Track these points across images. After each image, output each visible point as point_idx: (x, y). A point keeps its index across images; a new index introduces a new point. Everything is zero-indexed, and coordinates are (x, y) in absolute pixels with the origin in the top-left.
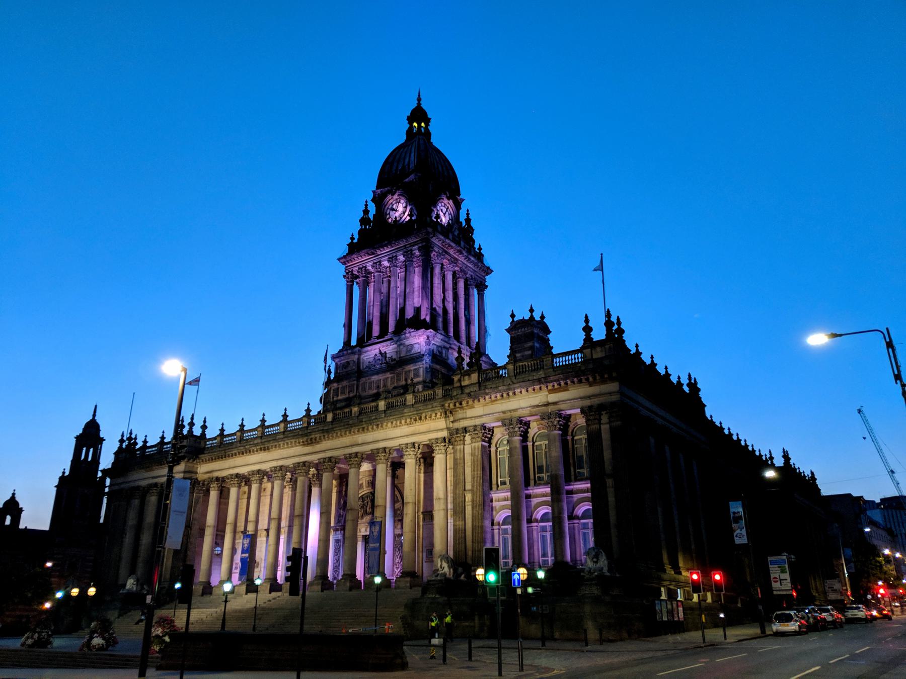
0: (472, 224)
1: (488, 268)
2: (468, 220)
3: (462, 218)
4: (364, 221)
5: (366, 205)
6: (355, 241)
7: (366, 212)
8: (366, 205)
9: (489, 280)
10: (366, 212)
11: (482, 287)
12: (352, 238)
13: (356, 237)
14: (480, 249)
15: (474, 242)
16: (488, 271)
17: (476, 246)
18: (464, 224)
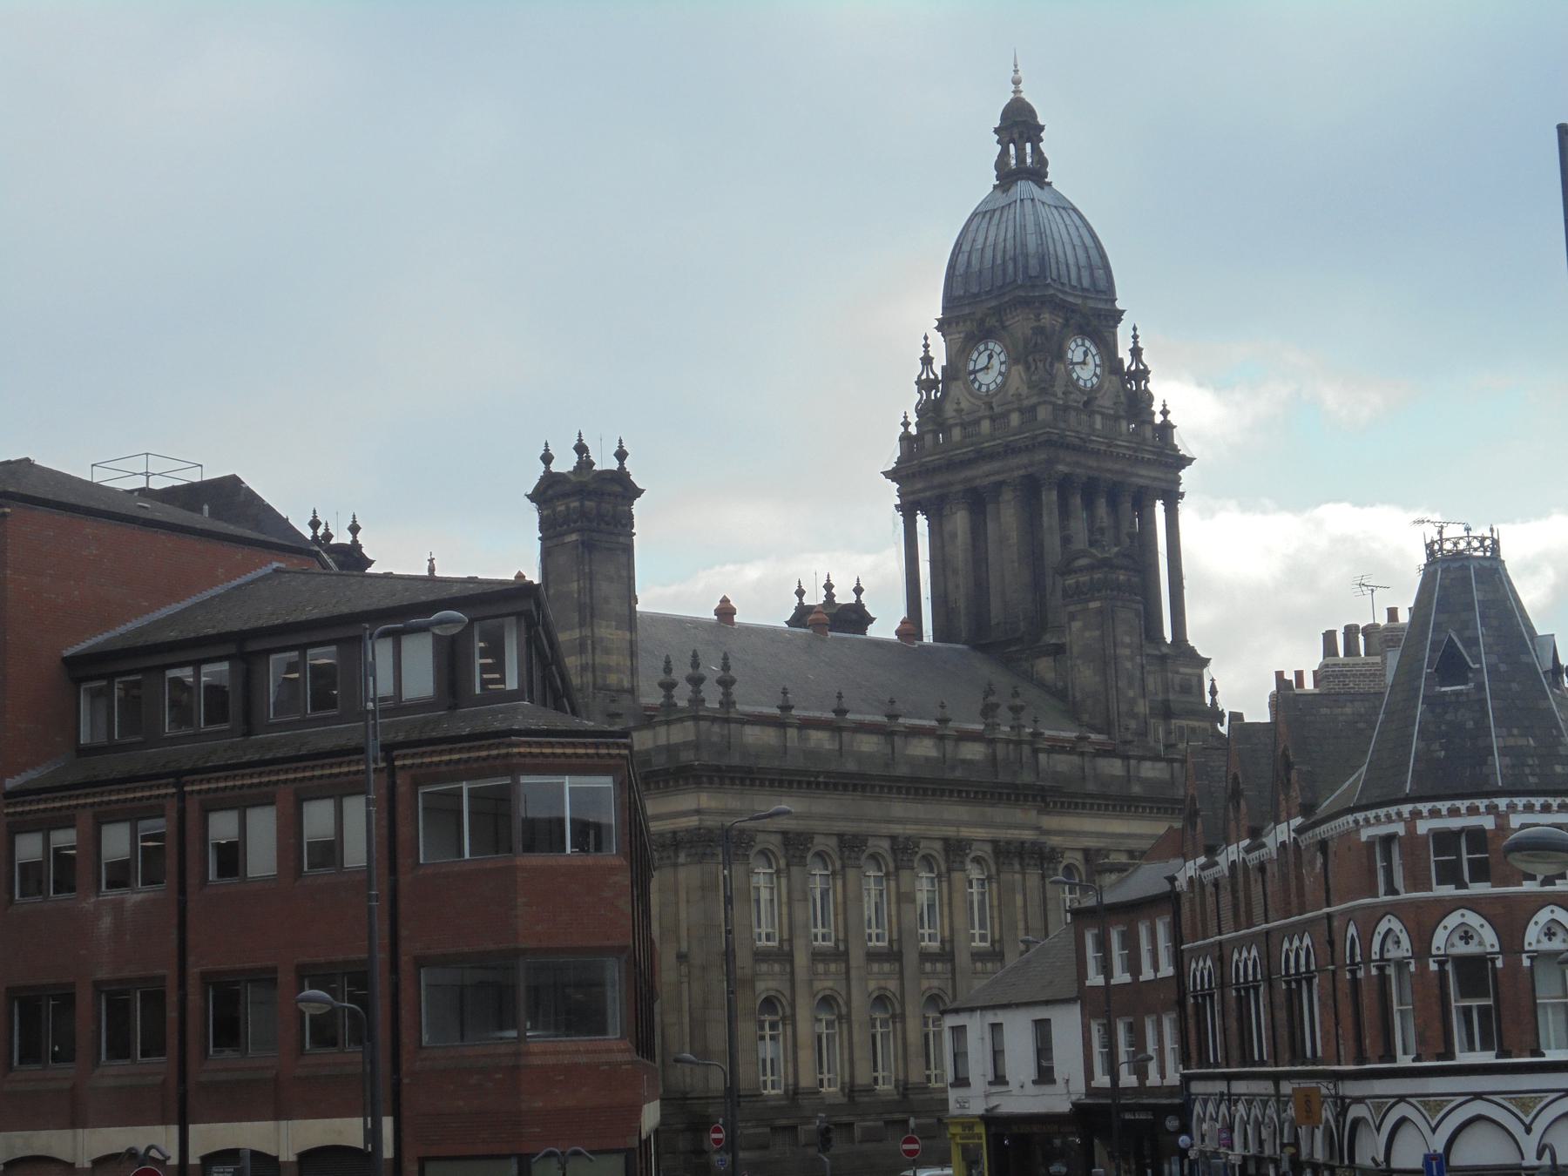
2: (1136, 352)
3: (1124, 354)
4: (925, 385)
5: (926, 346)
6: (913, 430)
7: (927, 361)
8: (926, 346)
9: (1187, 478)
10: (927, 361)
11: (1172, 499)
12: (906, 424)
13: (913, 419)
14: (1165, 413)
15: (1151, 398)
17: (1157, 407)
18: (1126, 364)
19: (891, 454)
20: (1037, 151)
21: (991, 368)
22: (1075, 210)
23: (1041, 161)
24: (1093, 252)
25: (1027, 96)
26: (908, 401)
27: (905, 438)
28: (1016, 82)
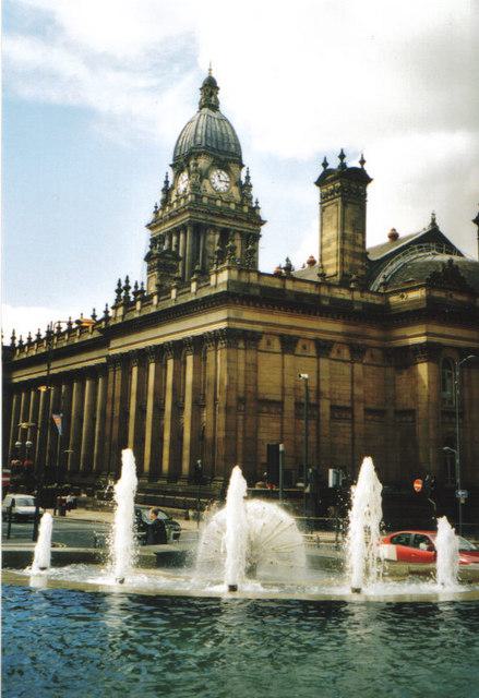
0: (252, 181)
1: (260, 220)
2: (248, 178)
10: (167, 182)
12: (156, 207)
13: (159, 205)
14: (257, 203)
16: (262, 223)
17: (254, 201)
19: (150, 217)
20: (216, 98)
21: (184, 183)
22: (226, 120)
23: (217, 101)
24: (232, 138)
25: (214, 75)
26: (158, 197)
27: (156, 212)
28: (210, 70)
